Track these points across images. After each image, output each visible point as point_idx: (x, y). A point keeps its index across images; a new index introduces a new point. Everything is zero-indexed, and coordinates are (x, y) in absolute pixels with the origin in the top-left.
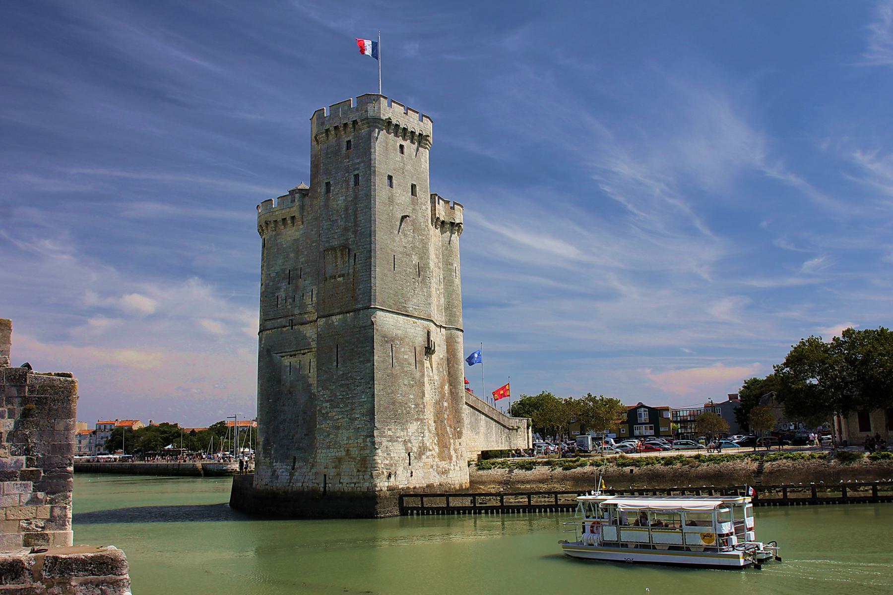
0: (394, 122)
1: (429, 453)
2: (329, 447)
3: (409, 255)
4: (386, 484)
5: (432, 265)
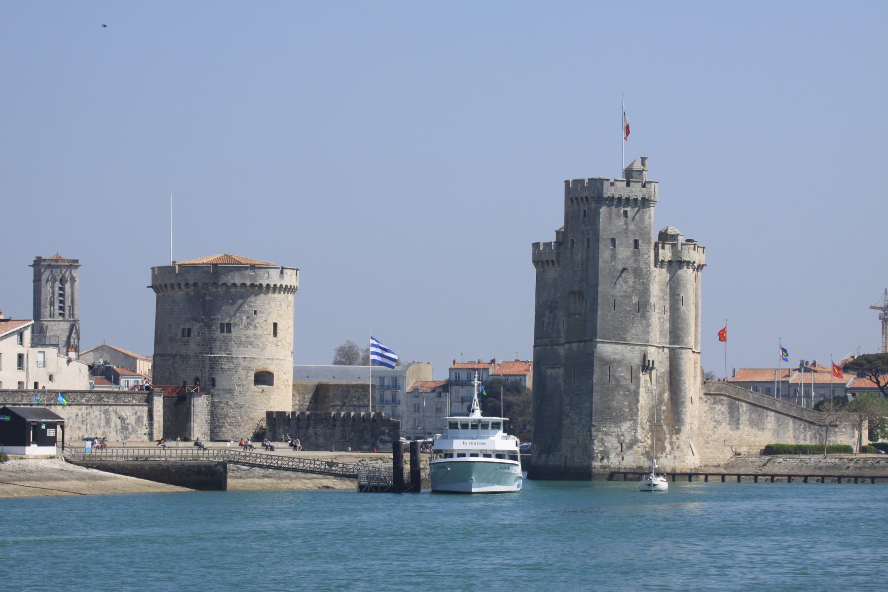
0: (617, 196)
1: (640, 444)
2: (568, 438)
3: (630, 297)
4: (599, 464)
5: (653, 300)
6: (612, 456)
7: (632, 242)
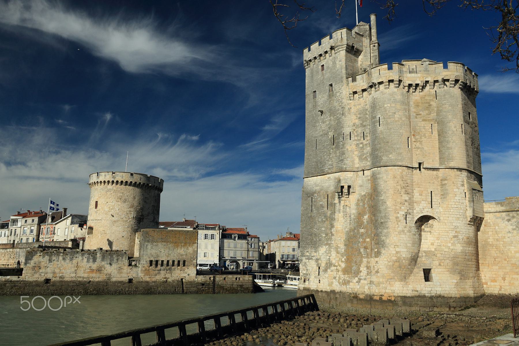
1: (333, 268)
3: (327, 134)
5: (347, 130)
6: (312, 278)
7: (327, 88)
